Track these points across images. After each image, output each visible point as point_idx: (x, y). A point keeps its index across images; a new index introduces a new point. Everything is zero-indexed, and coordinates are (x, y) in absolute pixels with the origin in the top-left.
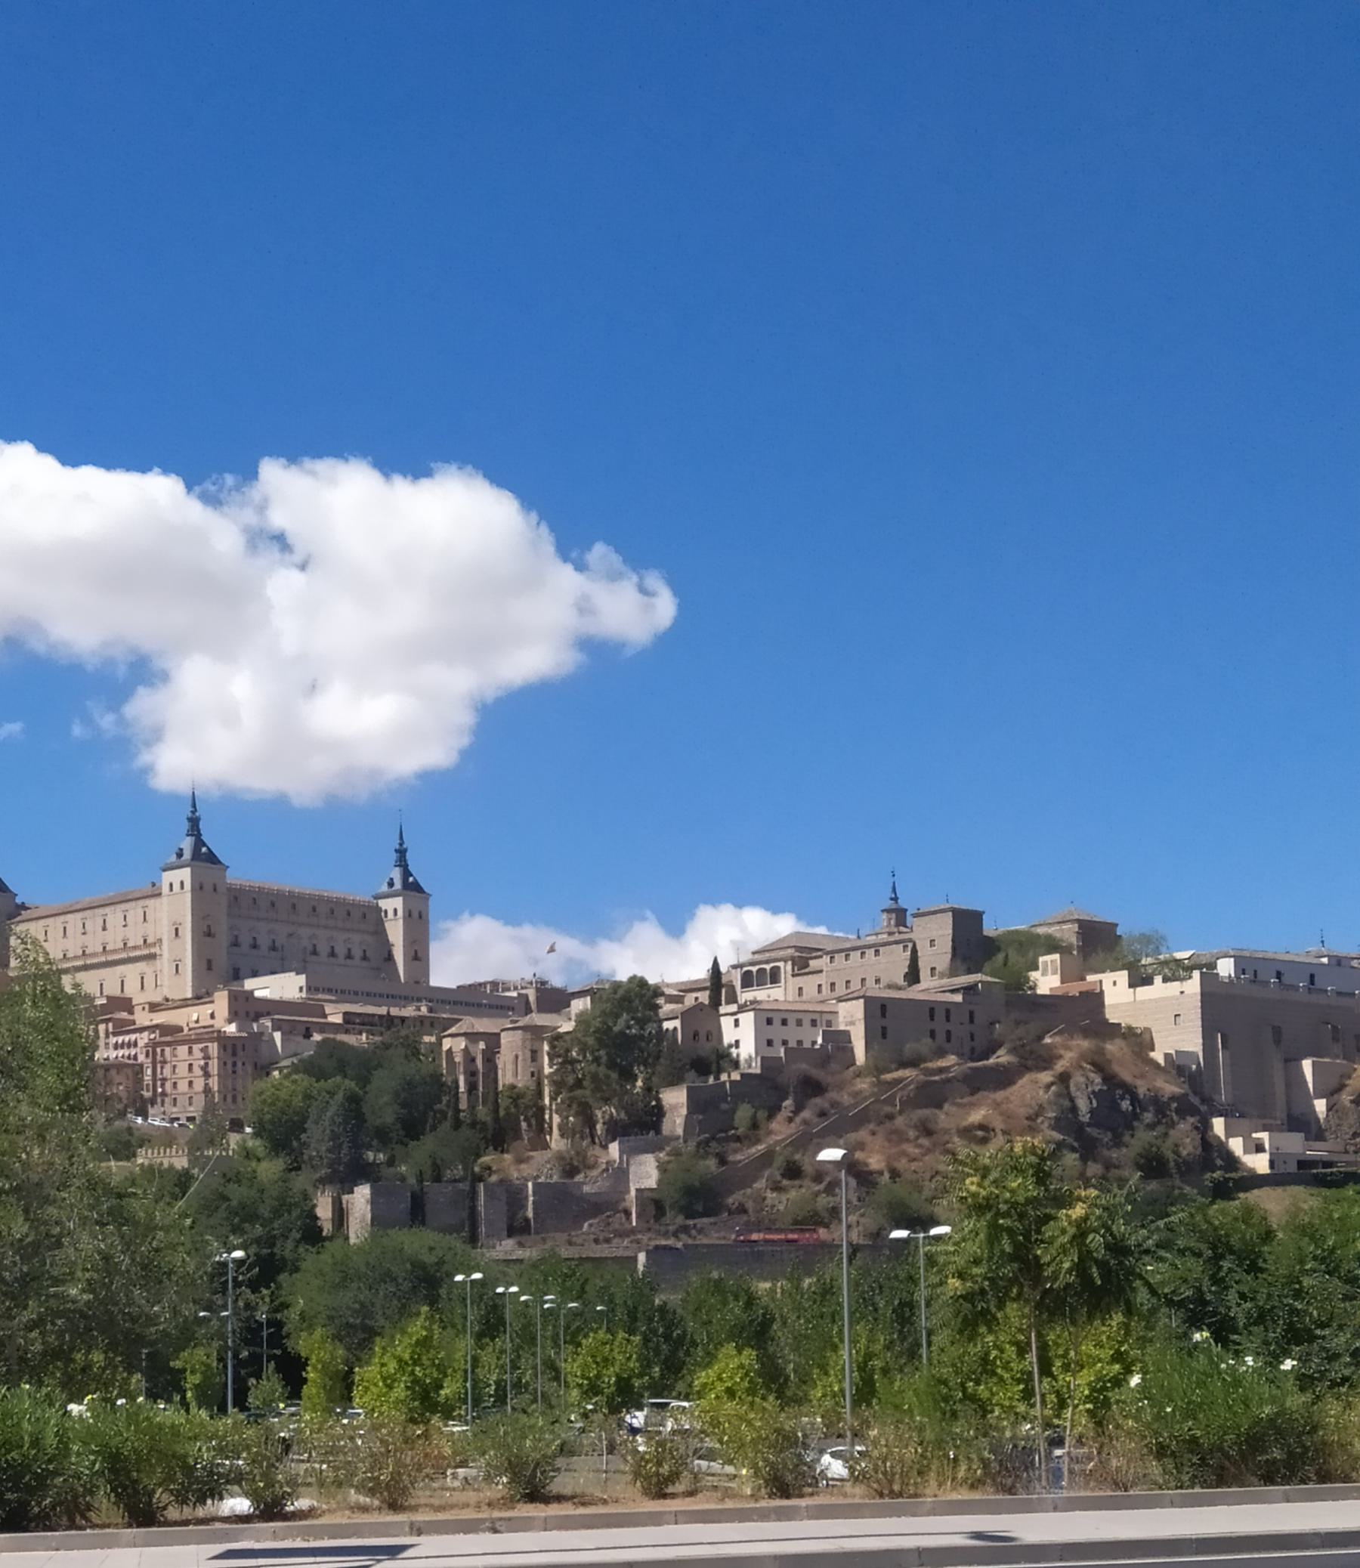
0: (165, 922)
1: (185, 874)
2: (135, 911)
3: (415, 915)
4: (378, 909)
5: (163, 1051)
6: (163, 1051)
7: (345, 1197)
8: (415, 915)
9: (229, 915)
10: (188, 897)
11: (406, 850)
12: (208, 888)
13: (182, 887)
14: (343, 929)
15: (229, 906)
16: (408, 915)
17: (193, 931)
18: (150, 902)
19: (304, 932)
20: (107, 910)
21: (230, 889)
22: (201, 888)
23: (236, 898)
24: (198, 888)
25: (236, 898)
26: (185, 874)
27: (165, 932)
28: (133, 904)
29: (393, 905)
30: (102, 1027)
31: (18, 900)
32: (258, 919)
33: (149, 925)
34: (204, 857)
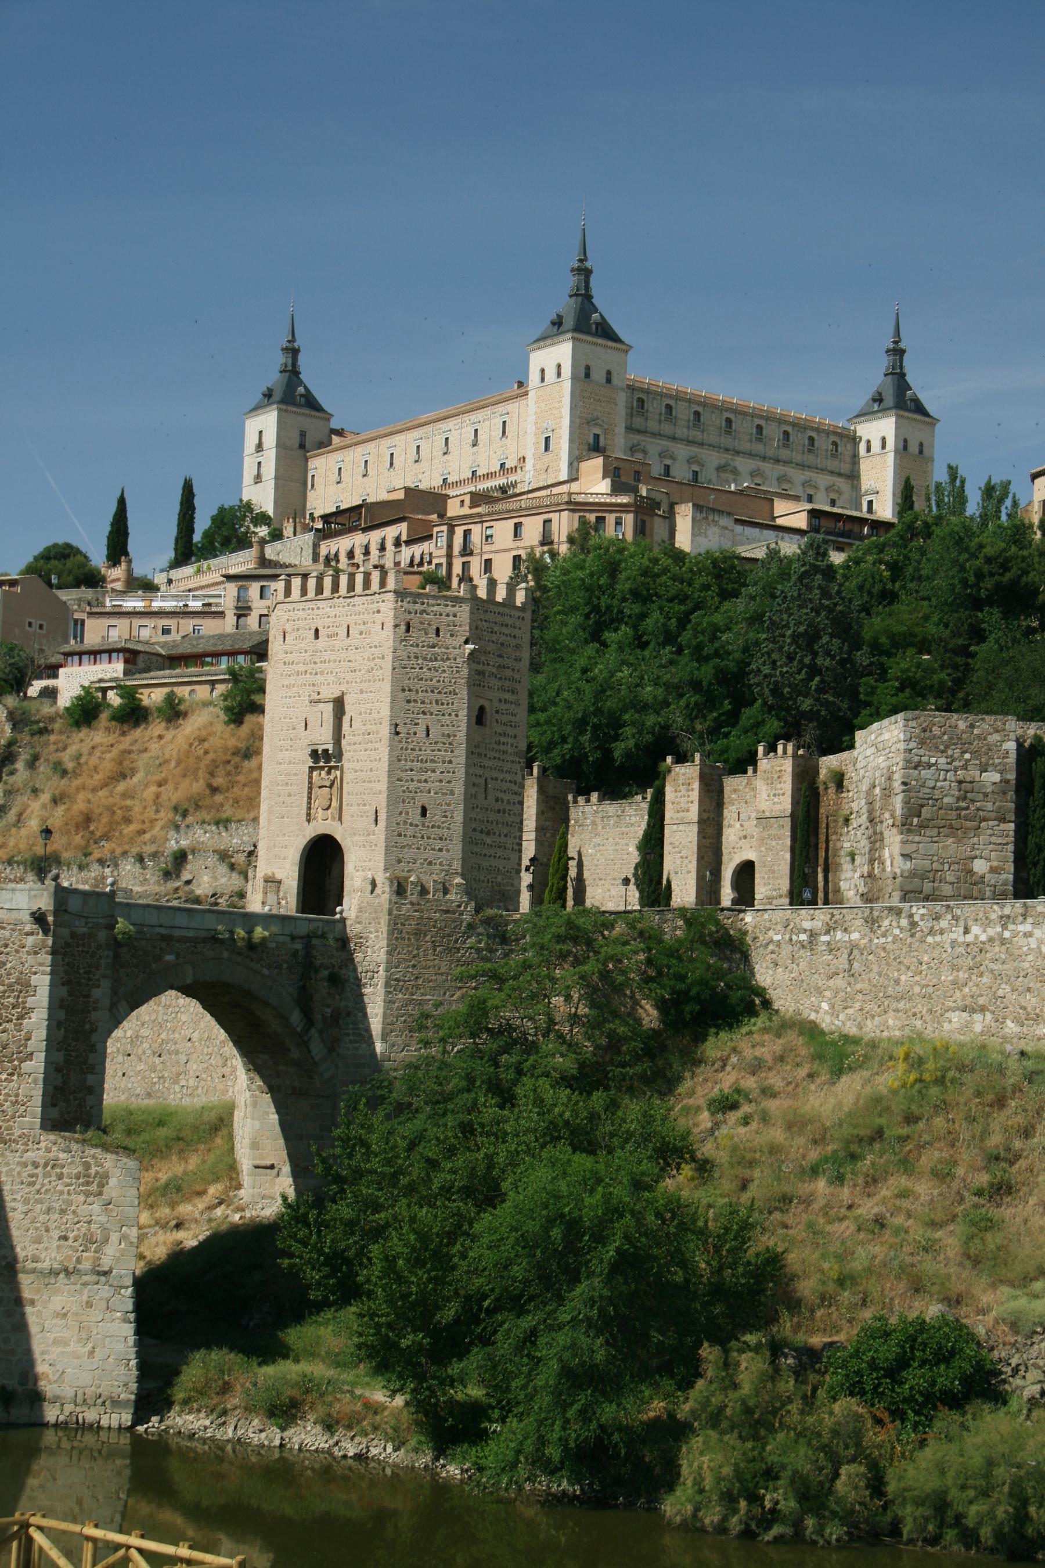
0: (531, 428)
1: (561, 353)
2: (488, 422)
3: (913, 448)
4: (855, 440)
5: (467, 534)
6: (467, 534)
7: (828, 763)
8: (913, 448)
9: (629, 429)
10: (567, 385)
11: (902, 352)
12: (598, 375)
13: (559, 375)
14: (802, 466)
15: (631, 415)
16: (903, 447)
17: (571, 441)
18: (512, 407)
19: (744, 464)
20: (451, 424)
21: (632, 388)
22: (587, 375)
23: (641, 401)
24: (583, 375)
25: (641, 401)
26: (561, 353)
27: (531, 448)
28: (487, 412)
29: (880, 431)
30: (391, 532)
31: (334, 424)
32: (674, 438)
33: (510, 441)
34: (588, 324)
